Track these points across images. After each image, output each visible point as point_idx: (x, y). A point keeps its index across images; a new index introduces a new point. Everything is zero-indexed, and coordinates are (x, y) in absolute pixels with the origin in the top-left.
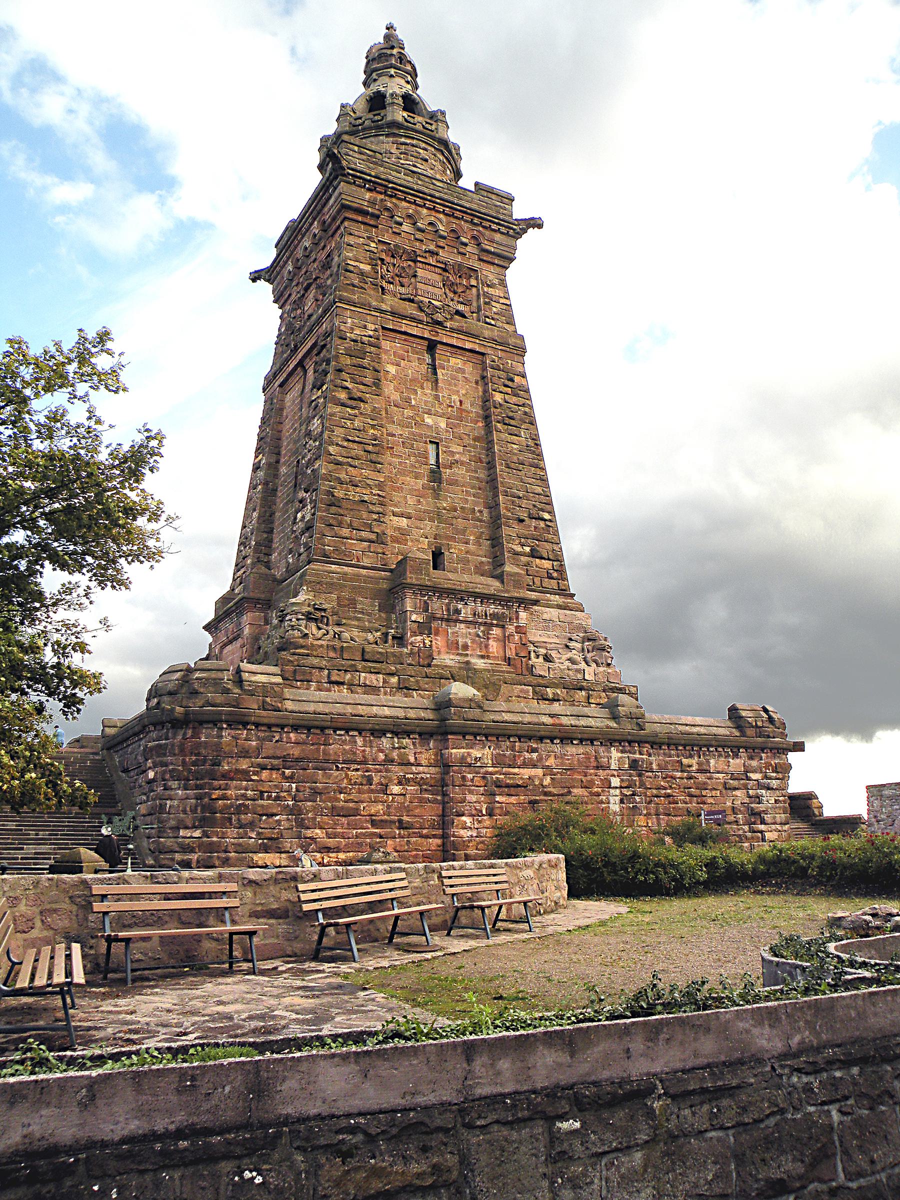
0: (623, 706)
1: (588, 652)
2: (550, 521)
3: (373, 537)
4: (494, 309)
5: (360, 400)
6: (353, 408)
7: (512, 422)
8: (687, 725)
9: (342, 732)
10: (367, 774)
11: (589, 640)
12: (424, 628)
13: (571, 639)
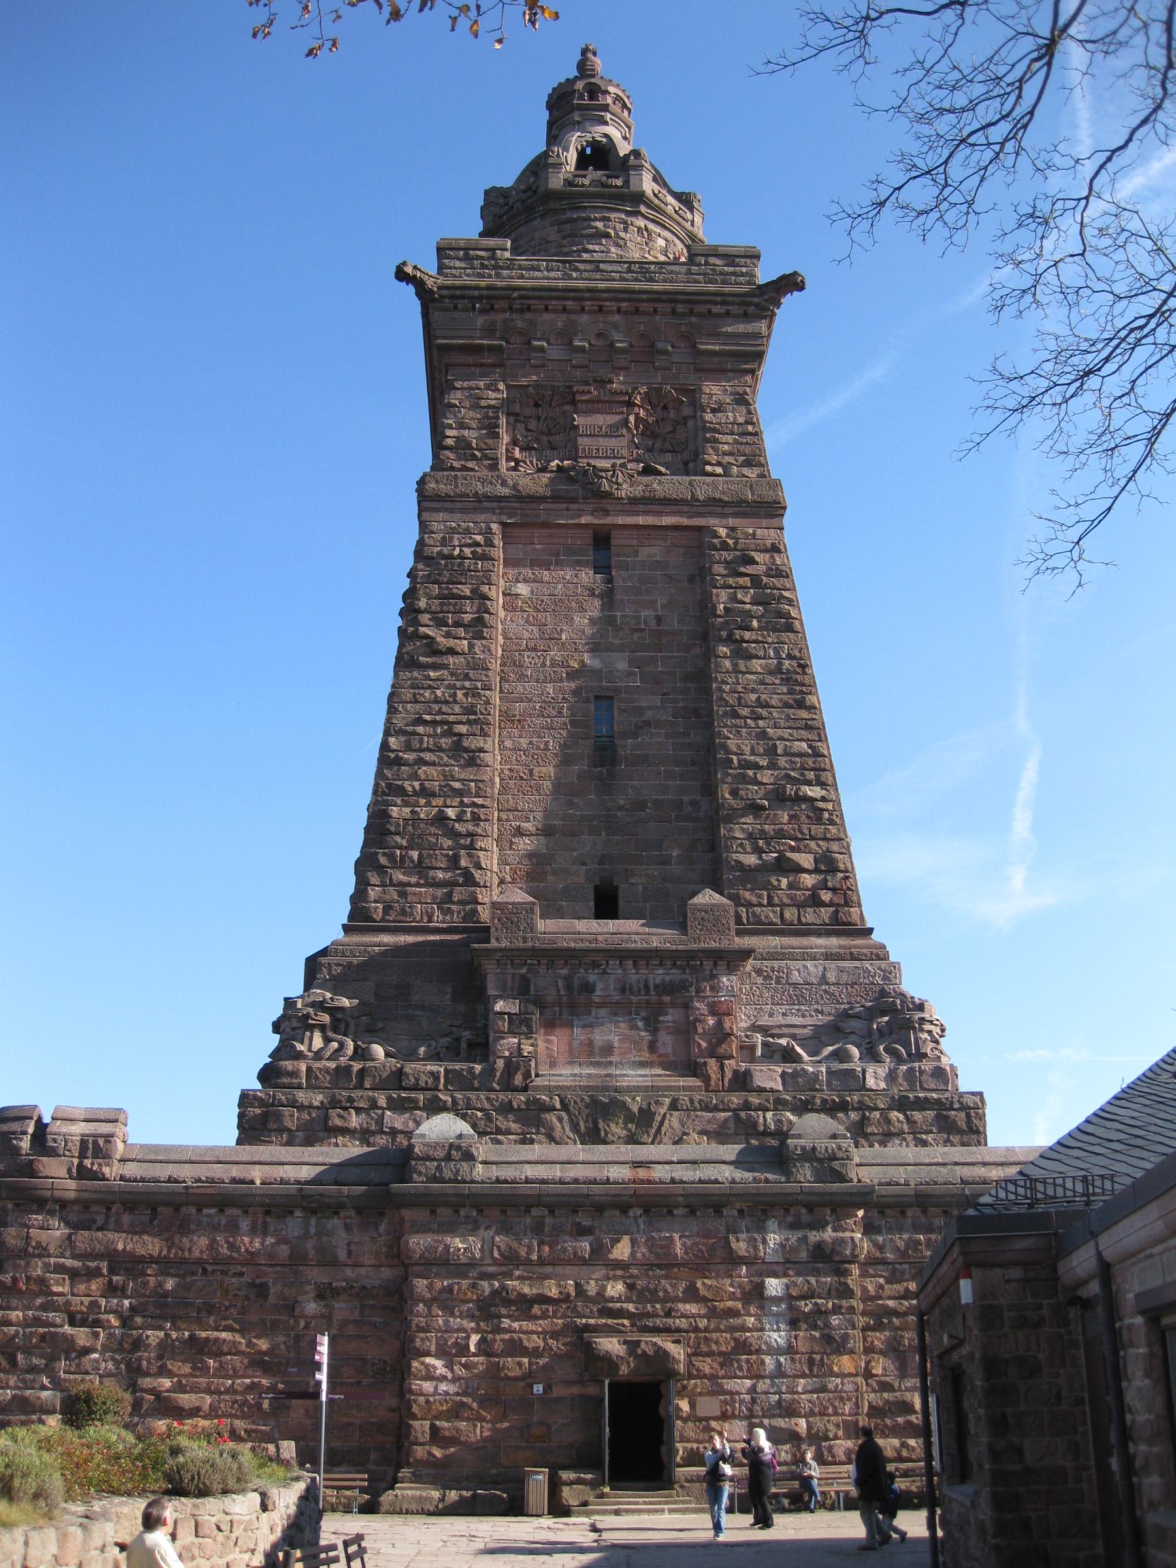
0: (799, 1136)
2: (823, 799)
5: (452, 651)
6: (436, 667)
8: (985, 1164)
9: (213, 1211)
12: (520, 1025)
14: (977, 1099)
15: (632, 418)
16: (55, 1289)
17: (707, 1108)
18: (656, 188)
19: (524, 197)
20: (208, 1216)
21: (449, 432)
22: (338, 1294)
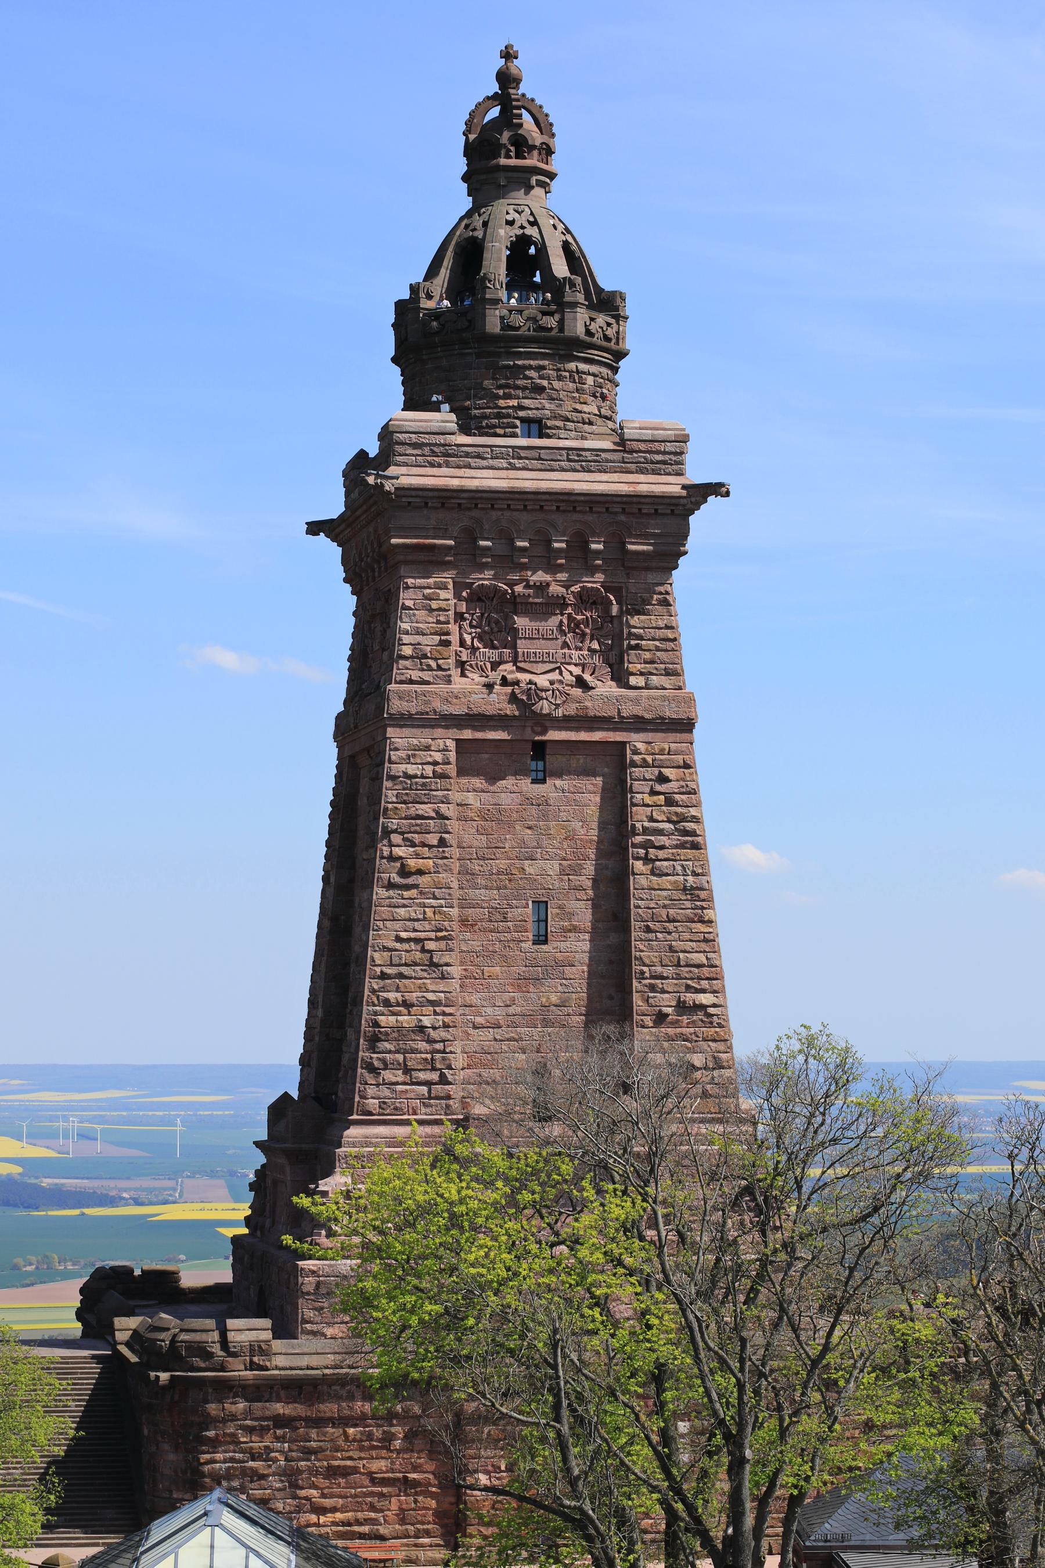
2: (714, 1006)
3: (435, 1076)
4: (647, 655)
5: (420, 872)
6: (408, 887)
10: (367, 1429)
15: (565, 621)
16: (242, 1440)
20: (335, 1390)
21: (406, 639)
22: (417, 1435)
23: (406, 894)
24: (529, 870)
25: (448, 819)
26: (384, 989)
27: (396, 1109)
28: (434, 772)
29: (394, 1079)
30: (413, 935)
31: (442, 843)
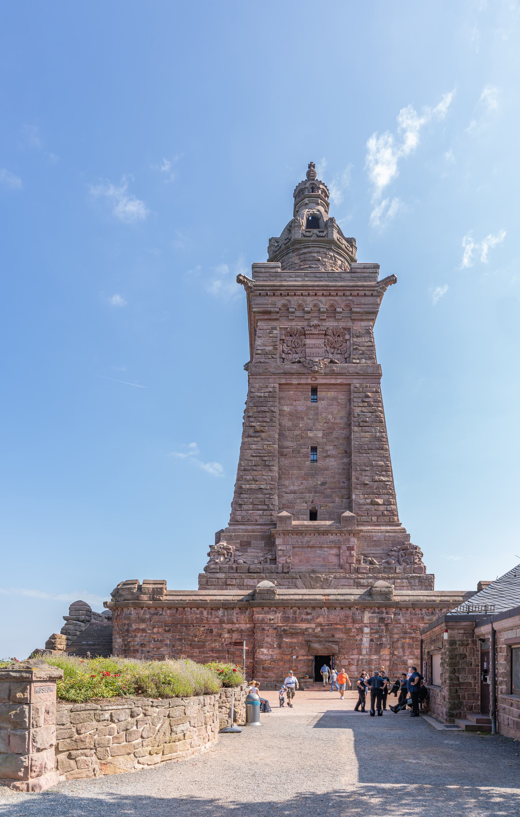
1: (402, 556)
3: (265, 507)
4: (361, 352)
6: (256, 437)
7: (365, 424)
11: (403, 550)
13: (392, 551)
14: (432, 576)
17: (345, 578)
18: (339, 236)
19: (286, 242)
23: (255, 439)
24: (309, 435)
25: (274, 412)
26: (245, 475)
27: (248, 519)
28: (269, 395)
29: (248, 509)
30: (258, 455)
31: (271, 420)
